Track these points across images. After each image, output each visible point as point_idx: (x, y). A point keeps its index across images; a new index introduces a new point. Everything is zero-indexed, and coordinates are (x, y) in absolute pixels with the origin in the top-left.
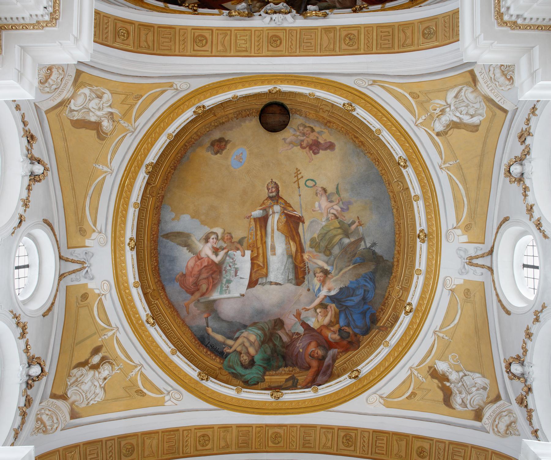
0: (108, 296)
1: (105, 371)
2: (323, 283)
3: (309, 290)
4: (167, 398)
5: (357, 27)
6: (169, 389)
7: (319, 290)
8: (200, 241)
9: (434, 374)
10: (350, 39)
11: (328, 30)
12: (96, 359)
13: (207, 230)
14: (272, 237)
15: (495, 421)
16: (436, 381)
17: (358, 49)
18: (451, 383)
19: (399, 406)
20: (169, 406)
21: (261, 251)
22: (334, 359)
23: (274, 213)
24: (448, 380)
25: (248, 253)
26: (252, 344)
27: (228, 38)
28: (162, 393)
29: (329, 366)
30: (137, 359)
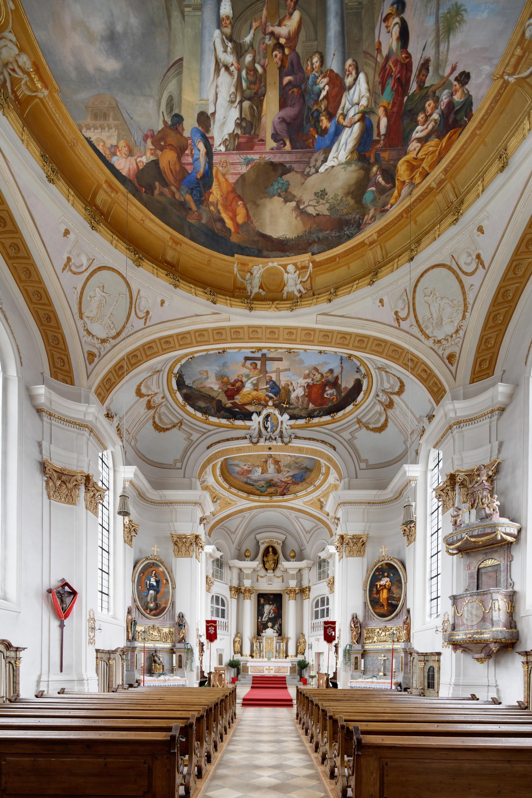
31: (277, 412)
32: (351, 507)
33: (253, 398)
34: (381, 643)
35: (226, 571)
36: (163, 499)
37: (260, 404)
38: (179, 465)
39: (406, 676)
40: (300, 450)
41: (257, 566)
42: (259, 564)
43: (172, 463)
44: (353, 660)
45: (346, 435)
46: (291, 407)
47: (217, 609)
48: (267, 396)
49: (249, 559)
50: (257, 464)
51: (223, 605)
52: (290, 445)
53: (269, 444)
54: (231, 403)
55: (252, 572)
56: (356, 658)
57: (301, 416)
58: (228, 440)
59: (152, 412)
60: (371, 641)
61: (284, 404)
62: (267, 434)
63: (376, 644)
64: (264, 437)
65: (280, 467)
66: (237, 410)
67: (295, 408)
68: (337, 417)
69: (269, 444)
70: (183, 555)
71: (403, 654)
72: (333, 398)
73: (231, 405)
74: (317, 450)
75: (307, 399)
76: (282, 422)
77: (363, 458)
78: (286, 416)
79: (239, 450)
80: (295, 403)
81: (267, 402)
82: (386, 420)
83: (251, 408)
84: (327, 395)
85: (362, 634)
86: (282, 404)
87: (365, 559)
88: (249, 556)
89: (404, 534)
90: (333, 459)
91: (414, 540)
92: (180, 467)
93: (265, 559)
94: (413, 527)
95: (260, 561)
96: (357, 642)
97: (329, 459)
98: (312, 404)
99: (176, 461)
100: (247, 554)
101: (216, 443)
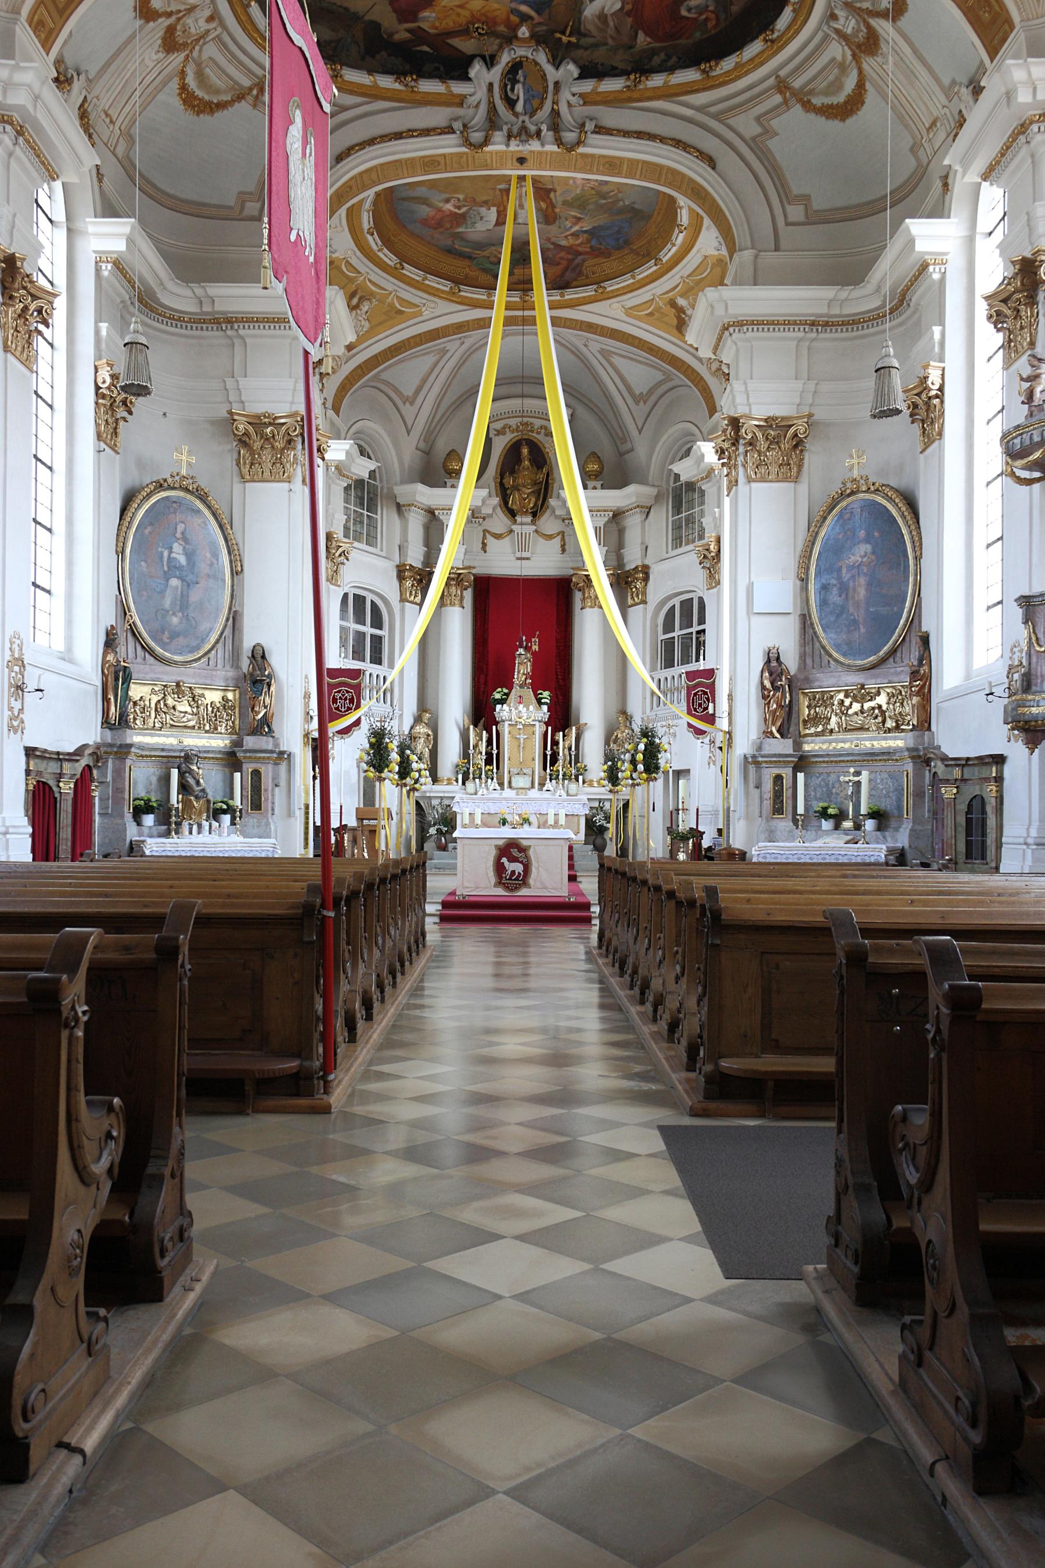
0: (353, 257)
1: (365, 307)
2: (575, 224)
5: (621, 160)
9: (673, 304)
11: (584, 156)
12: (355, 301)
13: (447, 196)
16: (674, 310)
19: (638, 318)
20: (427, 314)
22: (584, 261)
24: (684, 313)
25: (494, 209)
27: (465, 159)
29: (578, 265)
30: (390, 287)
31: (542, 57)
32: (761, 334)
33: (473, 16)
34: (849, 736)
35: (386, 519)
36: (207, 308)
37: (492, 33)
38: (252, 208)
39: (919, 828)
40: (613, 165)
41: (484, 501)
42: (490, 495)
43: (231, 201)
44: (768, 785)
45: (746, 124)
46: (584, 41)
47: (360, 636)
48: (513, 11)
50: (485, 198)
51: (377, 623)
52: (581, 150)
53: (520, 148)
54: (409, 31)
56: (778, 779)
57: (614, 68)
58: (398, 136)
59: (177, 59)
60: (820, 728)
61: (563, 33)
62: (513, 118)
63: (834, 737)
64: (505, 128)
65: (553, 206)
66: (426, 48)
67: (596, 46)
68: (718, 71)
69: (520, 148)
70: (267, 474)
71: (909, 767)
72: (706, 20)
73: (408, 35)
74: (661, 167)
75: (629, 20)
76: (557, 84)
77: (795, 191)
78: (572, 69)
79: (430, 164)
80: (594, 32)
81: (515, 28)
82: (860, 86)
83: (465, 45)
84: (689, 10)
85: (795, 708)
86: (558, 35)
87: (803, 488)
89: (911, 415)
90: (707, 193)
91: (940, 434)
92: (256, 213)
93: (509, 481)
94: (937, 396)
95: (493, 485)
96: (778, 731)
97: (698, 193)
98: (646, 34)
99: (243, 197)
101: (363, 145)
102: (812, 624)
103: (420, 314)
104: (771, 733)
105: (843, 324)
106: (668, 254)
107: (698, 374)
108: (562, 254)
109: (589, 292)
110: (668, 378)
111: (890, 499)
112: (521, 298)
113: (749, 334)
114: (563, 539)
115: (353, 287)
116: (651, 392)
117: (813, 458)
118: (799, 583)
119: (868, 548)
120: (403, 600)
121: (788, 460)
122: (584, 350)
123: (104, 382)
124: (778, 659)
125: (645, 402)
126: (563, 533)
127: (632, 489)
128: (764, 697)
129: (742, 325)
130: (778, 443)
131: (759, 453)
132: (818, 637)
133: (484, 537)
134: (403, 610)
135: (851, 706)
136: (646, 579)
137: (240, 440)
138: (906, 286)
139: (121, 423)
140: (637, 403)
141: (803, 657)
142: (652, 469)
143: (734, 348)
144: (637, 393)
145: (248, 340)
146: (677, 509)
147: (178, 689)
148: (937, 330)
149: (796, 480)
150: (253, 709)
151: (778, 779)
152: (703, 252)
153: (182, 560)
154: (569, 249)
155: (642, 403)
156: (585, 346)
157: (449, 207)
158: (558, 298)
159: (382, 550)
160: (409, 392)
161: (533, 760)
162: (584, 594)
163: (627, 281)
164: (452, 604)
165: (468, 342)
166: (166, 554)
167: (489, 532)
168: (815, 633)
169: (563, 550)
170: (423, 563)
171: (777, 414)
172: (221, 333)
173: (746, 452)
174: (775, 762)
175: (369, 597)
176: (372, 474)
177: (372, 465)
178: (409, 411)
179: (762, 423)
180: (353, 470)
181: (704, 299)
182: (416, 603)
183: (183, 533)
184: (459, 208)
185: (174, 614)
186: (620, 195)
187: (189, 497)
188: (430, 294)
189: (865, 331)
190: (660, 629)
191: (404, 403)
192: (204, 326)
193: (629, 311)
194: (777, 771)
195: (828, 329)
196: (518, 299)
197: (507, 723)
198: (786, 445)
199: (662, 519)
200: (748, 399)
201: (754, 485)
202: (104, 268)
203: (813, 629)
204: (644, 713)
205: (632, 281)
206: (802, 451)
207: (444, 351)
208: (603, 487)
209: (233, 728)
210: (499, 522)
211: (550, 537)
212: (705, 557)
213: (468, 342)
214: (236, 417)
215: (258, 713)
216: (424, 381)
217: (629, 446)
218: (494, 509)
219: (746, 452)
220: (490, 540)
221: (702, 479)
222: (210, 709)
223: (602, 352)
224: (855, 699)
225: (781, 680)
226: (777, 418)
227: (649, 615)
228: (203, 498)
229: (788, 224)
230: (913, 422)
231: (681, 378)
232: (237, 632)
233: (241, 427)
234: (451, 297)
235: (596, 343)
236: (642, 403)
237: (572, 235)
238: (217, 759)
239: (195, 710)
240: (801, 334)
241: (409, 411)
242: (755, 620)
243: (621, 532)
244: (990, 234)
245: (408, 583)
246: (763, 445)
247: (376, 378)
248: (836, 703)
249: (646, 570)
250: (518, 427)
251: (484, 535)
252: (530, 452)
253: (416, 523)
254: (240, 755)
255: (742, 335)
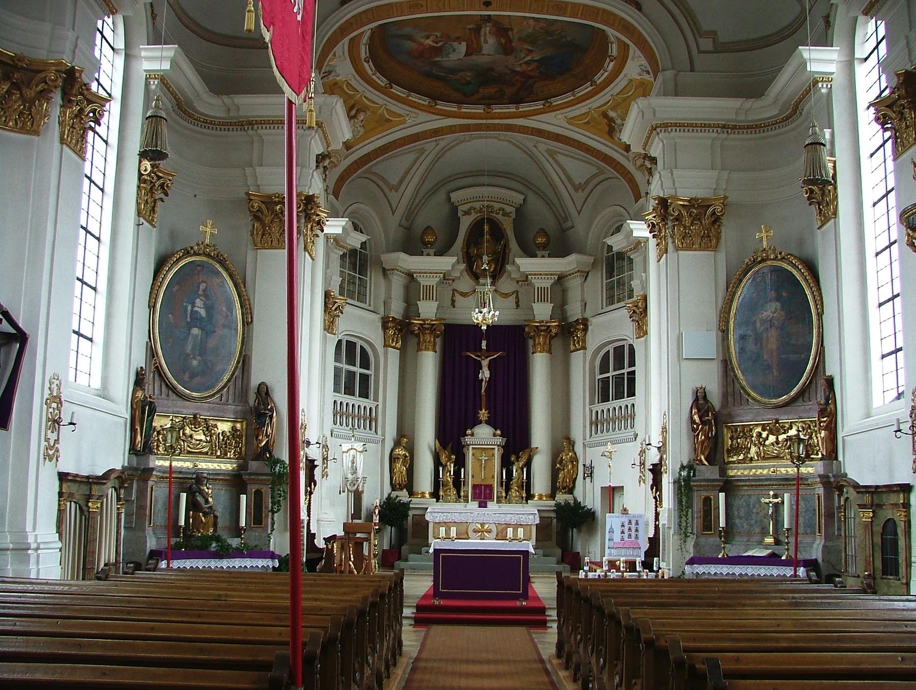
0: (353, 79)
1: (361, 116)
2: (527, 55)
3: (516, 57)
4: (407, 118)
6: (408, 113)
7: (525, 57)
8: (422, 38)
9: (605, 115)
10: (558, 8)
12: (353, 112)
13: (427, 33)
14: (485, 36)
15: (636, 157)
17: (564, 13)
18: (616, 124)
19: (577, 126)
21: (475, 42)
23: (486, 27)
24: (614, 123)
25: (464, 44)
26: (468, 77)
28: (404, 116)
30: (381, 102)
35: (374, 281)
41: (453, 266)
42: (458, 262)
49: (432, 251)
50: (457, 35)
51: (365, 364)
55: (440, 283)
88: (432, 244)
100: (430, 239)
102: (733, 368)
103: (404, 122)
104: (701, 460)
105: (748, 127)
106: (600, 78)
107: (626, 169)
108: (518, 77)
109: (539, 105)
110: (601, 172)
111: (794, 266)
112: (484, 110)
113: (673, 134)
114: (517, 297)
115: (352, 102)
116: (587, 182)
117: (729, 232)
118: (720, 333)
119: (778, 305)
120: (386, 345)
121: (708, 233)
122: (534, 149)
123: (146, 170)
124: (705, 397)
125: (583, 190)
126: (517, 292)
127: (573, 258)
128: (694, 430)
129: (668, 127)
130: (699, 219)
131: (685, 227)
132: (738, 379)
133: (453, 295)
134: (386, 353)
135: (767, 438)
136: (585, 330)
137: (254, 215)
138: (799, 98)
139: (159, 203)
140: (576, 190)
141: (725, 396)
142: (589, 242)
143: (661, 144)
144: (577, 183)
145: (264, 138)
146: (610, 274)
147: (195, 421)
148: (827, 132)
149: (715, 248)
150: (257, 438)
151: (707, 501)
152: (629, 77)
153: (203, 312)
154: (522, 74)
155: (580, 190)
156: (535, 147)
157: (429, 42)
158: (514, 110)
159: (370, 306)
160: (394, 182)
161: (493, 477)
162: (535, 341)
163: (568, 97)
164: (427, 349)
165: (442, 144)
166: (189, 308)
167: (457, 291)
168: (736, 376)
169: (518, 306)
170: (403, 316)
171: (699, 196)
172: (244, 133)
173: (674, 226)
174: (705, 486)
175: (359, 343)
176: (363, 245)
177: (363, 238)
178: (394, 196)
179: (685, 203)
180: (348, 242)
181: (636, 105)
182: (397, 348)
183: (204, 291)
184: (437, 43)
185: (194, 358)
186: (564, 34)
187: (211, 261)
188: (411, 106)
189: (766, 134)
190: (597, 370)
191: (391, 190)
192: (231, 128)
193: (570, 121)
194: (705, 494)
195: (736, 131)
196: (482, 111)
197: (471, 447)
198: (706, 222)
199: (597, 282)
200: (674, 184)
201: (680, 252)
202: (152, 83)
203: (734, 372)
204: (584, 439)
205: (573, 98)
206: (719, 226)
207: (422, 151)
208: (549, 256)
209: (240, 453)
210: (465, 284)
211: (506, 296)
212: (634, 312)
213: (442, 144)
214: (252, 197)
215: (261, 441)
216: (407, 173)
217: (569, 224)
218: (461, 273)
219: (674, 226)
220: (458, 298)
221: (631, 250)
222: (221, 438)
223: (548, 151)
224: (771, 432)
225: (708, 416)
226: (698, 200)
227: (588, 358)
228: (222, 263)
229: (700, 52)
230: (810, 204)
231: (611, 172)
232: (246, 373)
233: (256, 205)
234: (429, 110)
235: (544, 145)
236: (580, 190)
237: (526, 63)
238: (226, 480)
239: (208, 439)
240: (715, 135)
241: (394, 196)
242: (684, 364)
243: (564, 292)
244: (866, 59)
245: (391, 332)
246: (687, 221)
247: (368, 171)
248: (755, 435)
249: (585, 322)
250: (481, 209)
251: (453, 294)
252: (490, 229)
253: (398, 283)
254: (246, 477)
255: (667, 134)
